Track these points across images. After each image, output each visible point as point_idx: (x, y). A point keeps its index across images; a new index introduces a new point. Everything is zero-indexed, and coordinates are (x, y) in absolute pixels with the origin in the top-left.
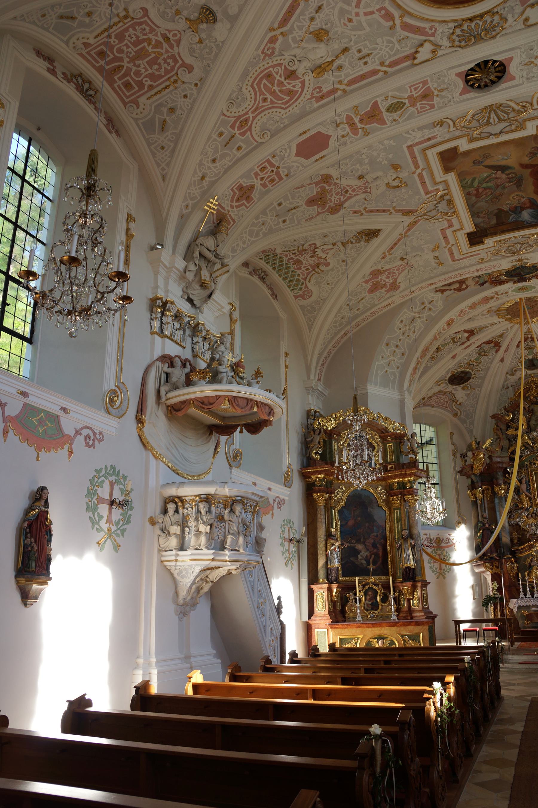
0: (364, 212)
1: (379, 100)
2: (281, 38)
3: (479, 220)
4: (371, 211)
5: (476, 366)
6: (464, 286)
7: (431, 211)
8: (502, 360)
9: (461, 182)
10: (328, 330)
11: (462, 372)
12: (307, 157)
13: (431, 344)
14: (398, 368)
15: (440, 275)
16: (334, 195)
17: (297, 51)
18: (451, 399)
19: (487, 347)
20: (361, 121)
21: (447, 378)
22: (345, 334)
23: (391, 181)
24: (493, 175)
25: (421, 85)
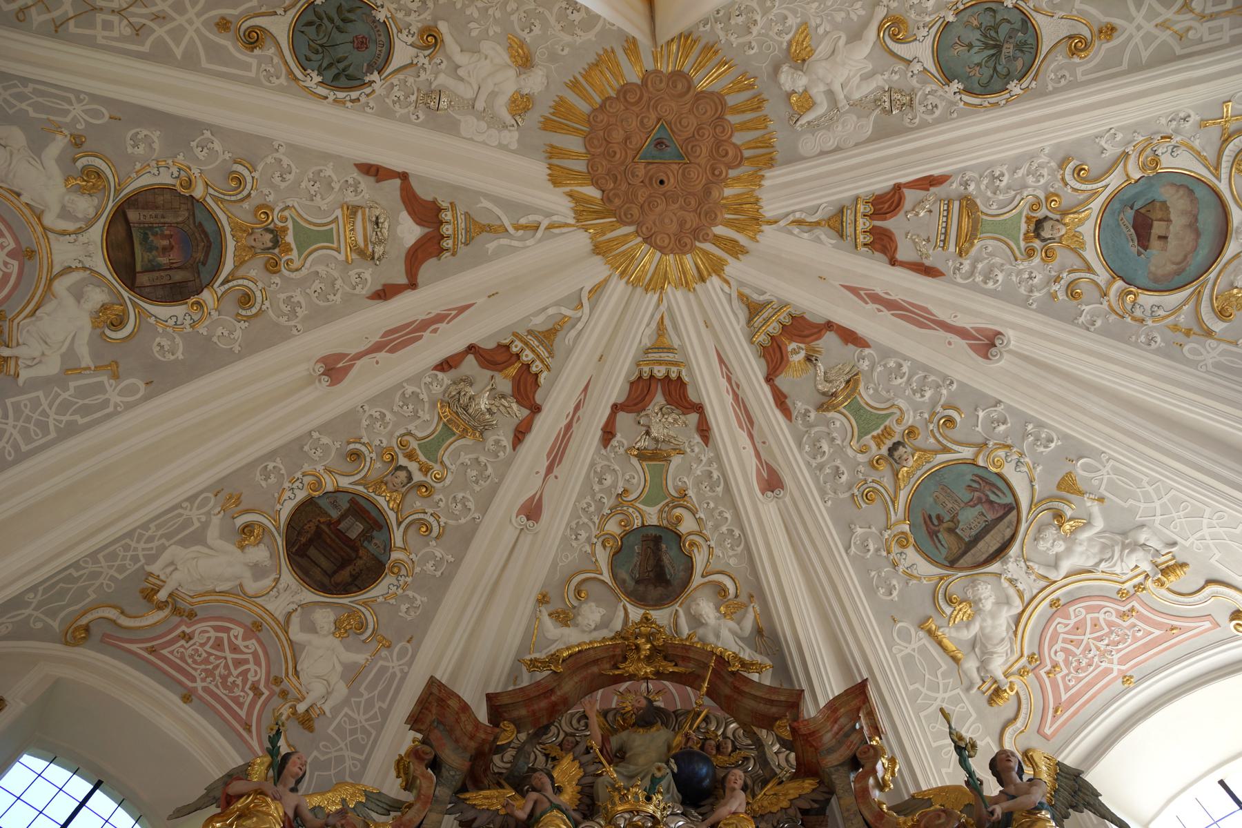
5: (421, 485)
8: (532, 510)
18: (278, 681)
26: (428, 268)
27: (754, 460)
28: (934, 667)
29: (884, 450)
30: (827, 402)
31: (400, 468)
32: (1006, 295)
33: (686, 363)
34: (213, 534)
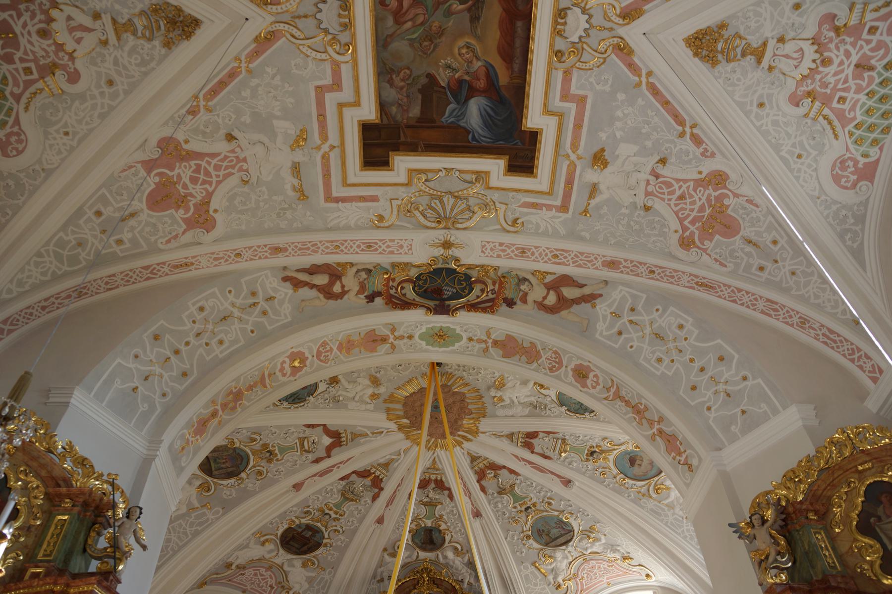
5: (335, 519)
8: (380, 521)
10: (39, 254)
11: (308, 527)
13: (250, 388)
14: (164, 395)
18: (280, 583)
19: (360, 484)
21: (279, 533)
26: (335, 451)
27: (471, 506)
29: (523, 509)
30: (501, 492)
31: (327, 514)
32: (577, 470)
33: (444, 474)
34: (251, 545)
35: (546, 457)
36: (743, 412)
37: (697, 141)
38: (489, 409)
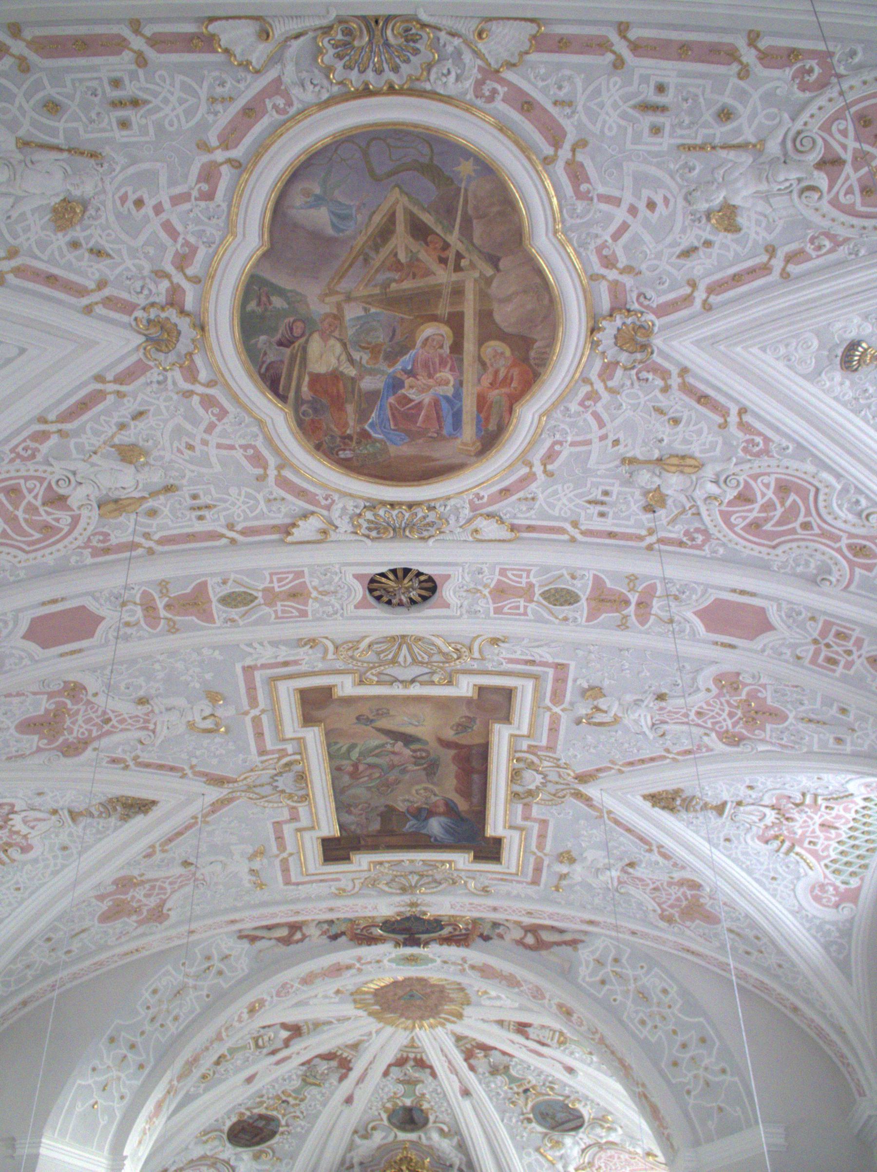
0: (131, 763)
1: (211, 582)
2: (54, 440)
3: (347, 818)
4: (147, 765)
5: (294, 1105)
6: (298, 936)
7: (262, 785)
8: (349, 1100)
9: (329, 746)
11: (261, 1117)
12: (44, 645)
13: (207, 1049)
14: (122, 1097)
15: (254, 907)
16: (80, 722)
17: (80, 466)
19: (323, 1066)
20: (168, 607)
21: (226, 1128)
22: (25, 1003)
23: (198, 719)
24: (389, 747)
25: (291, 576)
28: (542, 1166)
29: (521, 1090)
30: (494, 1071)
31: (284, 1102)
33: (424, 1051)
35: (543, 1044)
36: (720, 1109)
37: (665, 856)
38: (474, 998)
